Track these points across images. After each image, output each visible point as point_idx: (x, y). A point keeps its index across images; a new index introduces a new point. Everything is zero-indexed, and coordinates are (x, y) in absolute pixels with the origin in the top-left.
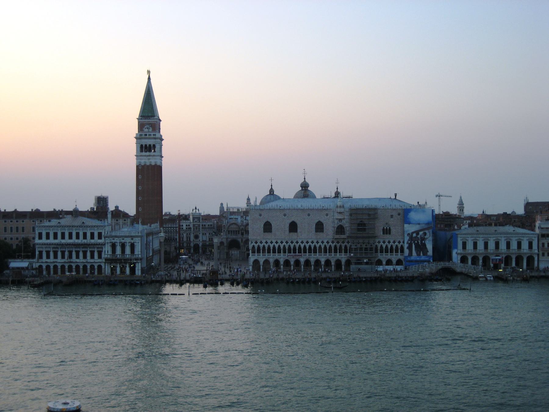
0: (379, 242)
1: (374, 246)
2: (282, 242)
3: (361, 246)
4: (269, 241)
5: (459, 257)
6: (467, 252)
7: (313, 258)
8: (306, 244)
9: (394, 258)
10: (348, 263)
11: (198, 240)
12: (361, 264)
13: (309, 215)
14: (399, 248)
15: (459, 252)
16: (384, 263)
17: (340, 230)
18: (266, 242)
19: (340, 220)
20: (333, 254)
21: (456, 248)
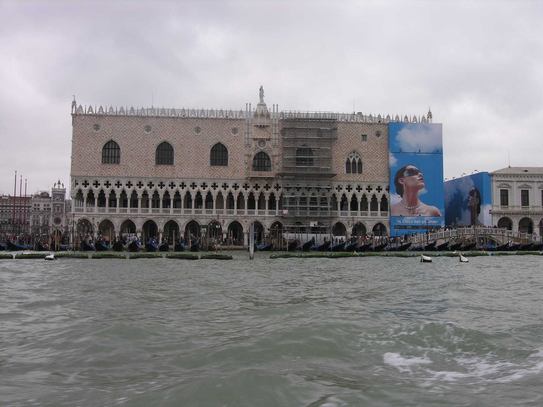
0: (339, 188)
1: (329, 195)
2: (140, 185)
3: (303, 194)
4: (113, 182)
6: (510, 209)
7: (204, 217)
8: (191, 189)
10: (277, 228)
11: (60, 225)
13: (198, 130)
14: (379, 200)
15: (495, 209)
17: (261, 161)
18: (108, 184)
20: (246, 210)
21: (490, 202)
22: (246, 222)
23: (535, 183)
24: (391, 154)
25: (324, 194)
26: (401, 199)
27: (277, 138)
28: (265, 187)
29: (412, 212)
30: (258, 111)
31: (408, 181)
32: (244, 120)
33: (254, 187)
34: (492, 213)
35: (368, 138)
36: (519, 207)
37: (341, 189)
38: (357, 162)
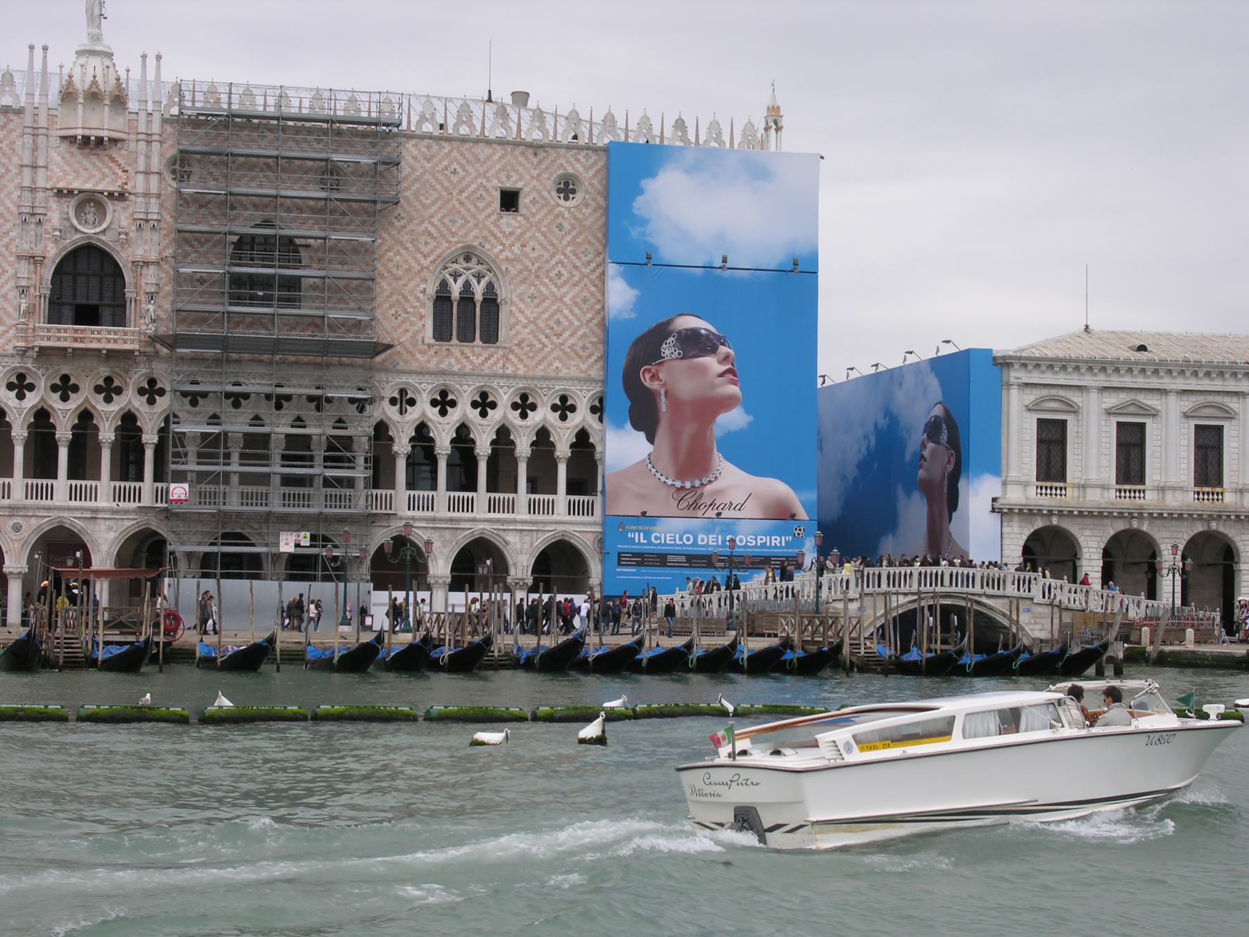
5: (1018, 535)
6: (1071, 498)
9: (524, 526)
10: (146, 553)
12: (247, 567)
14: (563, 449)
15: (1015, 496)
16: (440, 567)
19: (90, 202)
21: (995, 466)
22: (17, 528)
23: (1172, 398)
24: (612, 269)
25: (340, 422)
26: (649, 448)
27: (154, 189)
28: (98, 389)
29: (691, 499)
30: (77, 80)
31: (675, 377)
32: (20, 112)
33: (54, 388)
34: (1002, 511)
35: (524, 201)
36: (1104, 487)
37: (412, 402)
38: (479, 297)
